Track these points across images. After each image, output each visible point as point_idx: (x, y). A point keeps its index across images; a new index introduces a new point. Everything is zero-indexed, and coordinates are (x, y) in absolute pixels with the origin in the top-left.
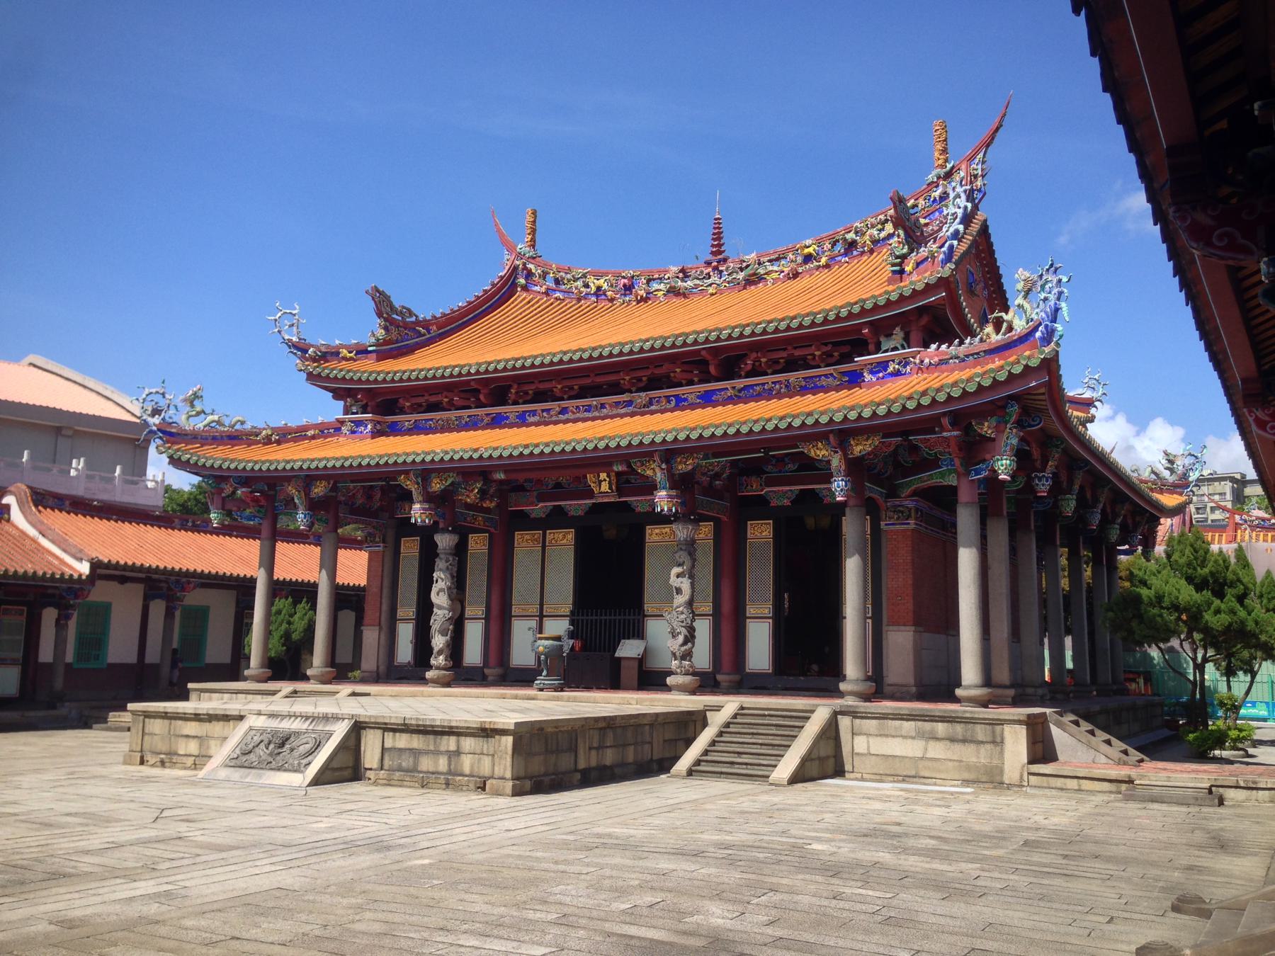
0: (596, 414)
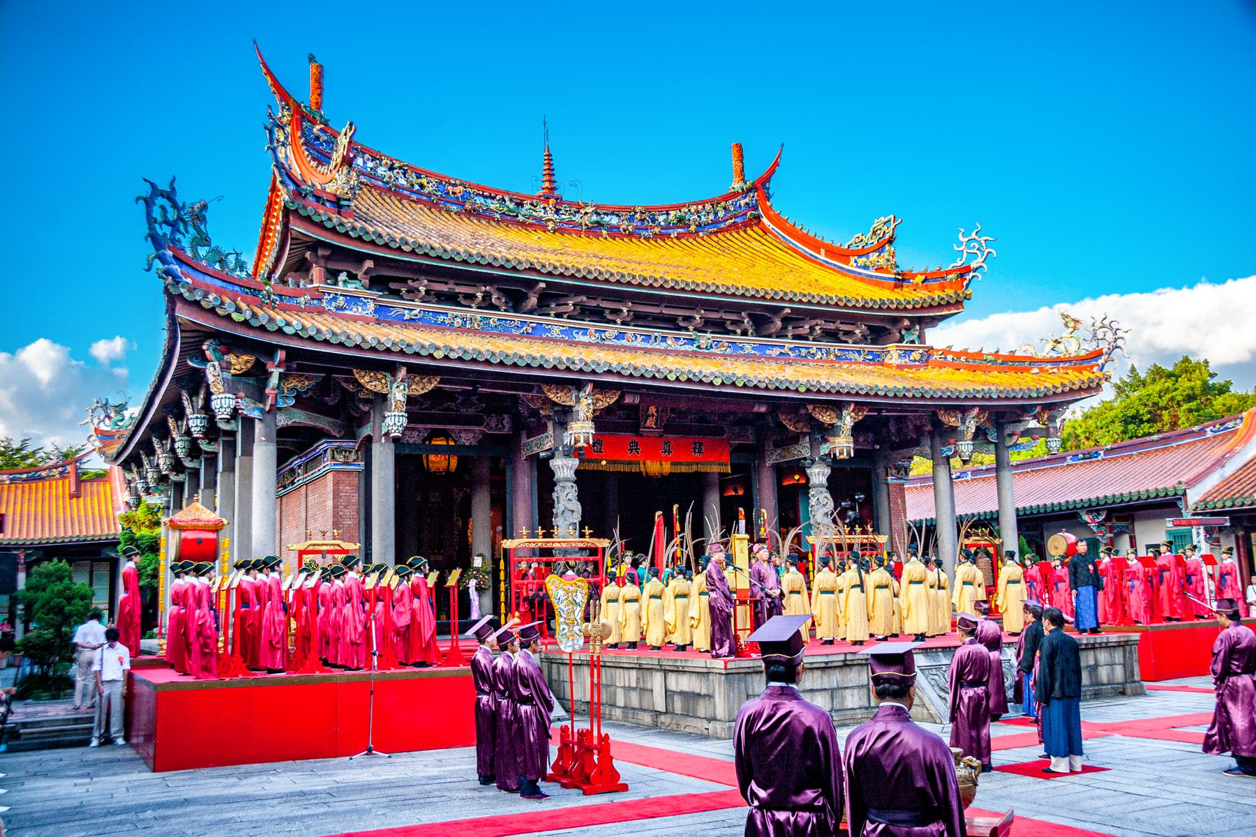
0: (655, 346)
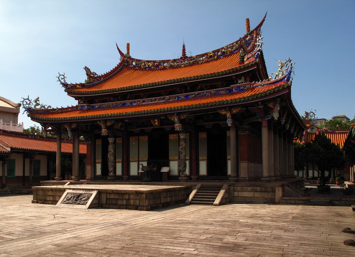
0: (154, 102)
